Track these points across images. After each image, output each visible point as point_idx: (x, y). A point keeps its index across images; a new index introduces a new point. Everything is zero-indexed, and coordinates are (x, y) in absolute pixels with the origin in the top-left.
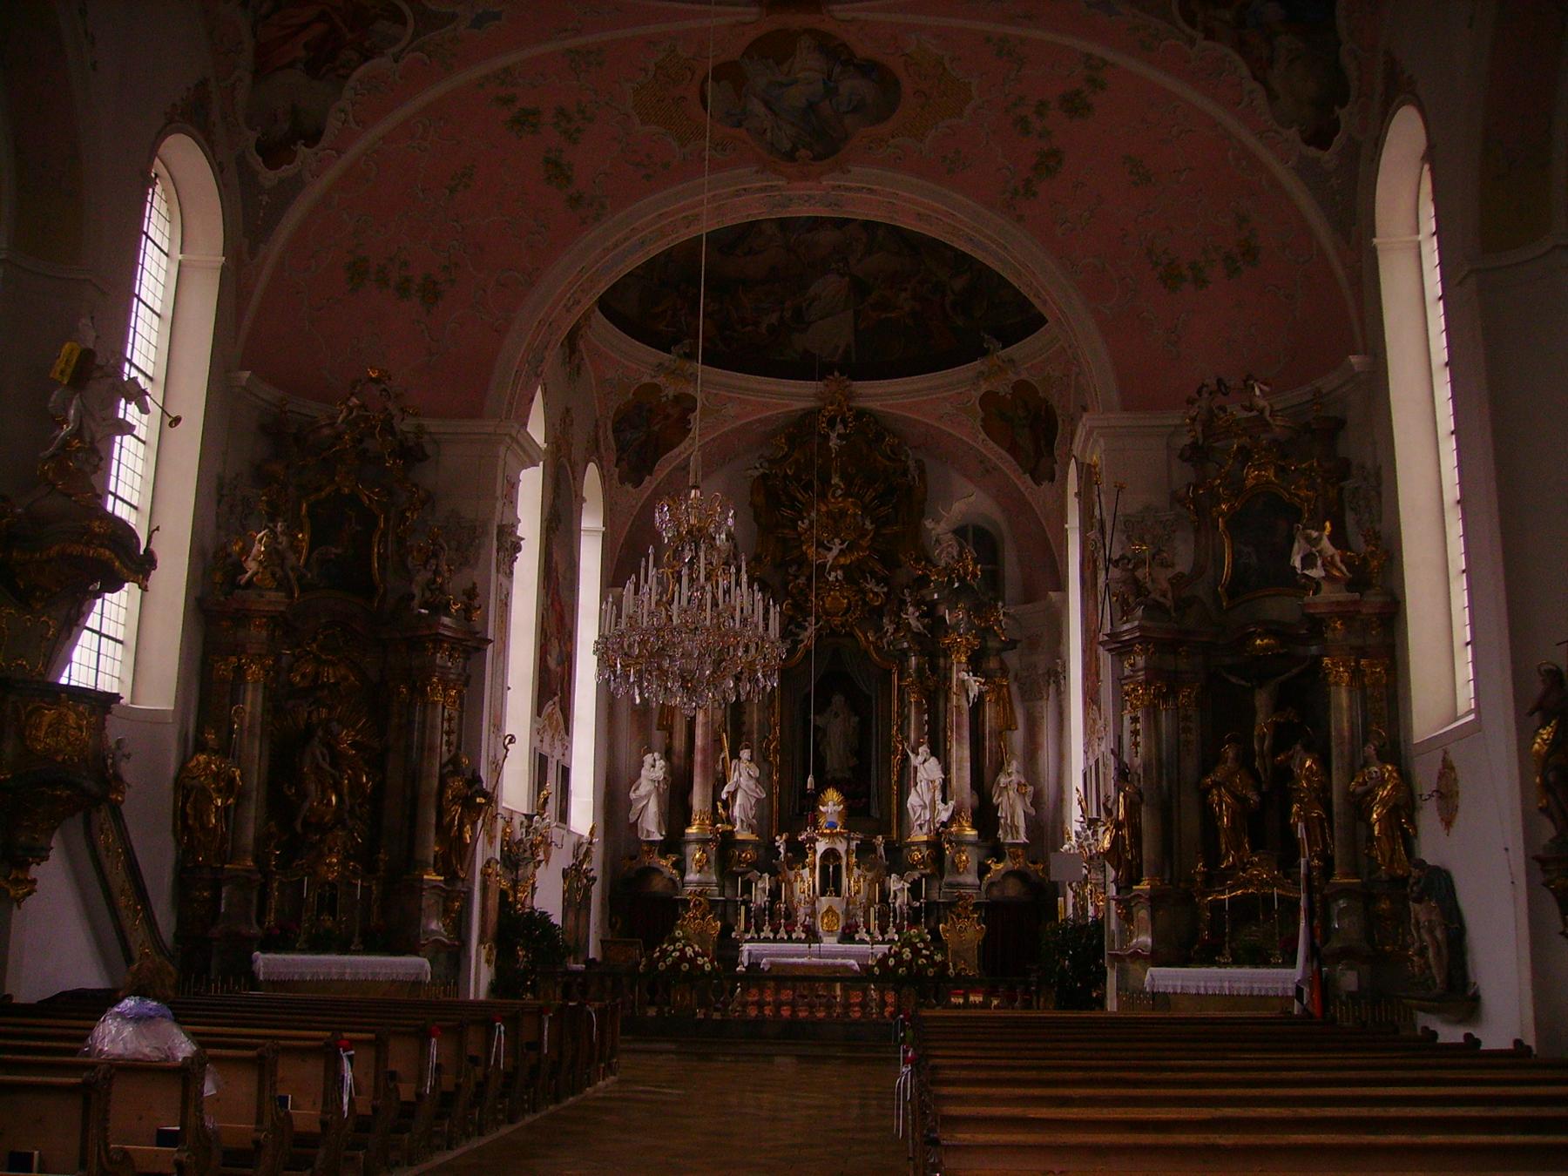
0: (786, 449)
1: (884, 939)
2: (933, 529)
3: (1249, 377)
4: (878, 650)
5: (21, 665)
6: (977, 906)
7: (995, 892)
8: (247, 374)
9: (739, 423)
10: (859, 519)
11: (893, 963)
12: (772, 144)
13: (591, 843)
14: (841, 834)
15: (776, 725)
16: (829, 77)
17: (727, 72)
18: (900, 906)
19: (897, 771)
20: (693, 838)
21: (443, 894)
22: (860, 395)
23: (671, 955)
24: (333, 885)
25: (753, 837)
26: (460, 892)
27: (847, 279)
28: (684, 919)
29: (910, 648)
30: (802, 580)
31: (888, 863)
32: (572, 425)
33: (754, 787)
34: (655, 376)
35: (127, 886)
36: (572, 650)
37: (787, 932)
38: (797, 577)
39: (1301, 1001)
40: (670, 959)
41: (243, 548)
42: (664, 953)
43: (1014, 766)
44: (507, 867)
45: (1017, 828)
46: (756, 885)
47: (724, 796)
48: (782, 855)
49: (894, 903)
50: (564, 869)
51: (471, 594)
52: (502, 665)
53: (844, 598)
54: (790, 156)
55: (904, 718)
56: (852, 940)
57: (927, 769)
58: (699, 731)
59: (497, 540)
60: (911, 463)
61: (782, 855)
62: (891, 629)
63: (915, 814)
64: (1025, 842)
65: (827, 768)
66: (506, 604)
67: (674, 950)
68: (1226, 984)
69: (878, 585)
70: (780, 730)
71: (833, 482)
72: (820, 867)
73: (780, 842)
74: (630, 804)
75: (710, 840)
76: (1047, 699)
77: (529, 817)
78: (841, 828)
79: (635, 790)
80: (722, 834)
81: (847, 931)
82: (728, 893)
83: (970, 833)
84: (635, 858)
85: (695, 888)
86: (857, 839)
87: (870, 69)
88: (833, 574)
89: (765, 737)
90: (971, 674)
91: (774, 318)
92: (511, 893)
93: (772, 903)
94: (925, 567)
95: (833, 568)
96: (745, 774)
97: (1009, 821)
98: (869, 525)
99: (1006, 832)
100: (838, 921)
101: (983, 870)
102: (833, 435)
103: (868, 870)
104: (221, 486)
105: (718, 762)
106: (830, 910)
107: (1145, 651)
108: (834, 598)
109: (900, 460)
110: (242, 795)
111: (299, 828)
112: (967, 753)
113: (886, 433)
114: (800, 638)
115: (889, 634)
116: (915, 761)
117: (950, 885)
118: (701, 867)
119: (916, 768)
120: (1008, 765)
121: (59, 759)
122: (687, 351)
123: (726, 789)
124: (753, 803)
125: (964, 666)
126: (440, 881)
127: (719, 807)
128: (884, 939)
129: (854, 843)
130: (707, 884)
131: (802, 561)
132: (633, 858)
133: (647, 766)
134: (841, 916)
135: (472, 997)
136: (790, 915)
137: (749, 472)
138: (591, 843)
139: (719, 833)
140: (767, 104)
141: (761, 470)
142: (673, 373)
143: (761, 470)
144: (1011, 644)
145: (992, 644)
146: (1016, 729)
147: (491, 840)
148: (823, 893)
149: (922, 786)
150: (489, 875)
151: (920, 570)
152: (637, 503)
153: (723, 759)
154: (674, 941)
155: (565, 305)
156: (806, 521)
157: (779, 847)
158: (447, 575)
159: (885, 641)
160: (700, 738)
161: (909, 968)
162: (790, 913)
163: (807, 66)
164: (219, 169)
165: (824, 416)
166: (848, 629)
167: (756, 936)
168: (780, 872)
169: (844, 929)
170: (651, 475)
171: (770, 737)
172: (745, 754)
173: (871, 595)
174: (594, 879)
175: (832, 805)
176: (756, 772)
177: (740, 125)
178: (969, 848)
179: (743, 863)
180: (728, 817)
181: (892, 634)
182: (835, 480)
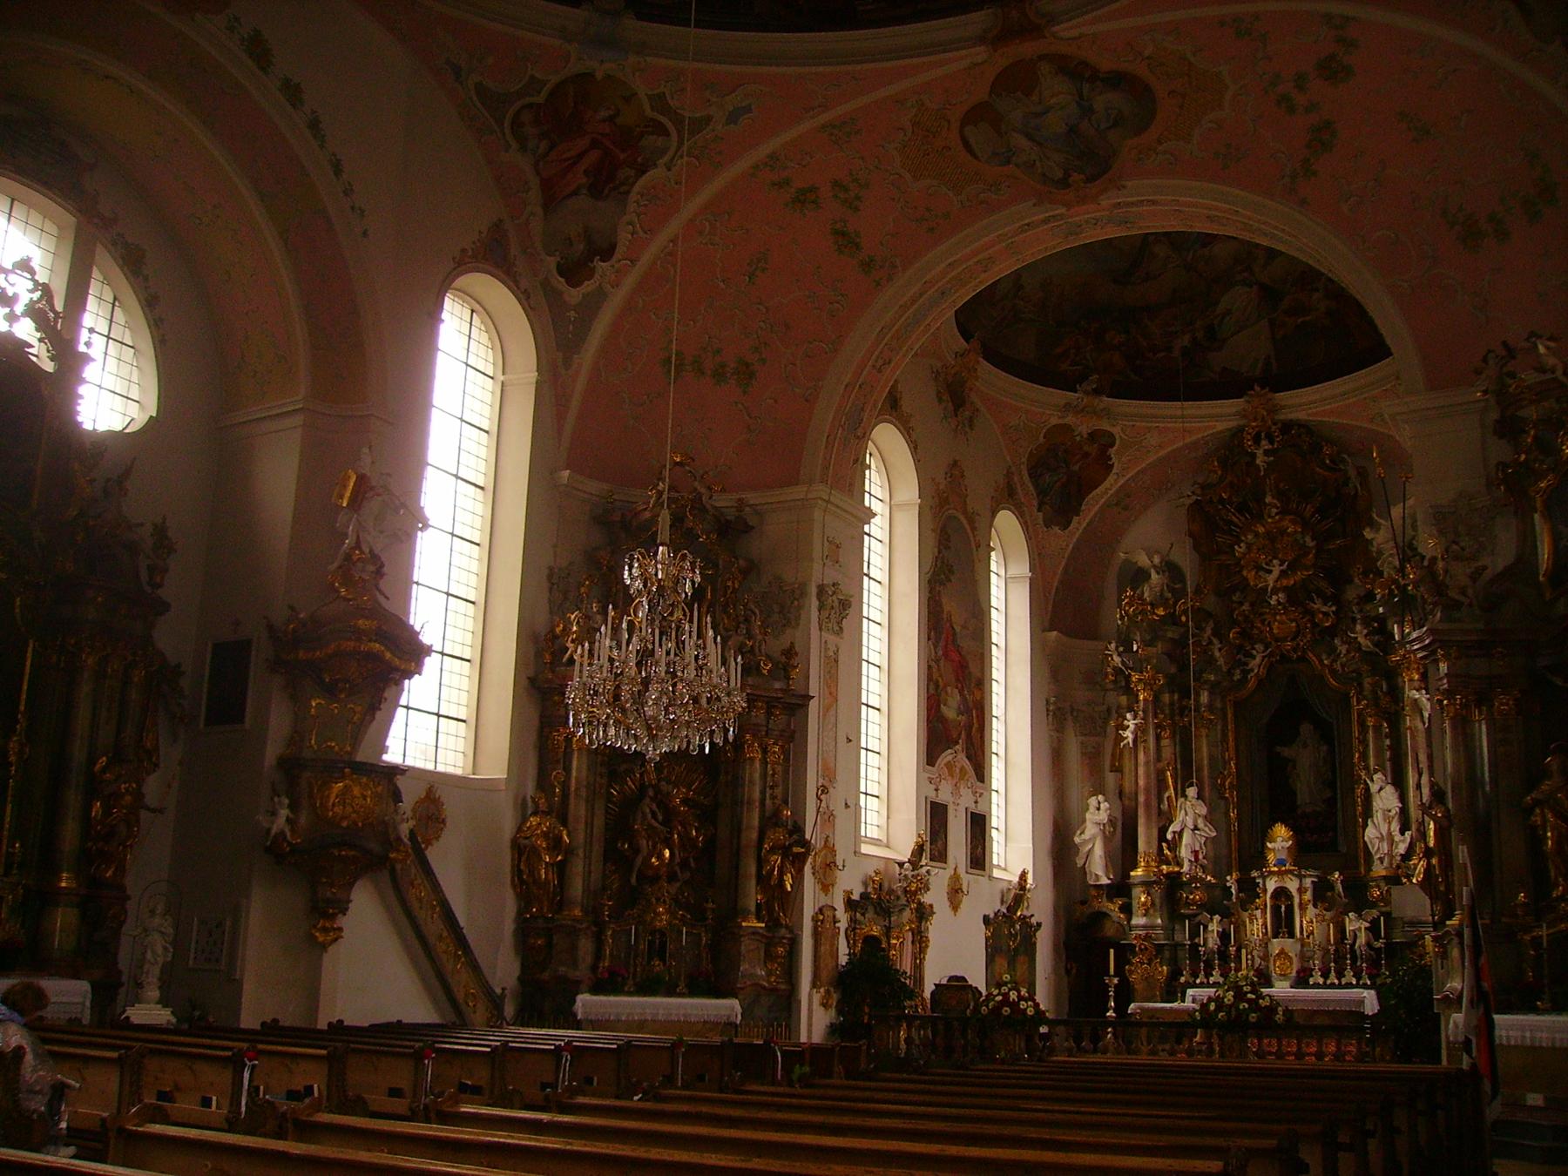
0: (1220, 472)
3: (1532, 334)
4: (1333, 672)
5: (330, 746)
8: (566, 473)
9: (1162, 453)
10: (1299, 536)
12: (1044, 175)
14: (1291, 872)
16: (1081, 96)
17: (978, 114)
20: (1136, 881)
21: (764, 940)
22: (1283, 407)
24: (663, 934)
26: (784, 938)
27: (1255, 287)
28: (1132, 964)
30: (1246, 607)
32: (963, 476)
34: (1063, 417)
35: (445, 934)
36: (983, 698)
38: (1241, 604)
39: (1469, 1053)
41: (564, 629)
44: (878, 915)
47: (1169, 836)
48: (1234, 897)
50: (985, 916)
51: (790, 652)
52: (833, 719)
53: (1292, 621)
54: (1064, 183)
56: (1305, 985)
57: (1385, 800)
59: (819, 599)
60: (1352, 473)
62: (1343, 649)
65: (1299, 803)
66: (836, 661)
67: (998, 995)
68: (1528, 1034)
69: (1325, 605)
70: (1236, 764)
71: (1267, 501)
72: (1271, 907)
73: (1231, 881)
74: (1075, 849)
75: (1155, 882)
77: (901, 865)
80: (1168, 875)
81: (1302, 975)
84: (1086, 903)
86: (1311, 876)
87: (1117, 80)
88: (1274, 597)
91: (1185, 340)
92: (884, 939)
95: (1275, 591)
100: (1291, 964)
102: (1260, 453)
103: (1326, 910)
104: (550, 577)
106: (1282, 952)
107: (1446, 657)
108: (1281, 622)
109: (1340, 470)
110: (569, 852)
111: (633, 881)
113: (1324, 443)
114: (1250, 666)
116: (1374, 788)
118: (1147, 910)
121: (344, 824)
123: (1171, 829)
125: (1416, 684)
126: (761, 928)
127: (1166, 845)
128: (1340, 983)
130: (1153, 927)
131: (1244, 586)
132: (1083, 903)
133: (1092, 809)
134: (1295, 960)
135: (803, 1039)
140: (1029, 136)
141: (1195, 497)
142: (1082, 410)
143: (1195, 497)
147: (826, 887)
148: (1275, 936)
149: (1378, 817)
150: (822, 921)
152: (1067, 546)
153: (1168, 798)
155: (874, 366)
158: (760, 637)
161: (1228, 1013)
163: (1056, 92)
164: (524, 298)
167: (1205, 981)
168: (1233, 914)
170: (1078, 515)
171: (1226, 773)
173: (1321, 616)
175: (1280, 839)
177: (1009, 163)
182: (1268, 500)
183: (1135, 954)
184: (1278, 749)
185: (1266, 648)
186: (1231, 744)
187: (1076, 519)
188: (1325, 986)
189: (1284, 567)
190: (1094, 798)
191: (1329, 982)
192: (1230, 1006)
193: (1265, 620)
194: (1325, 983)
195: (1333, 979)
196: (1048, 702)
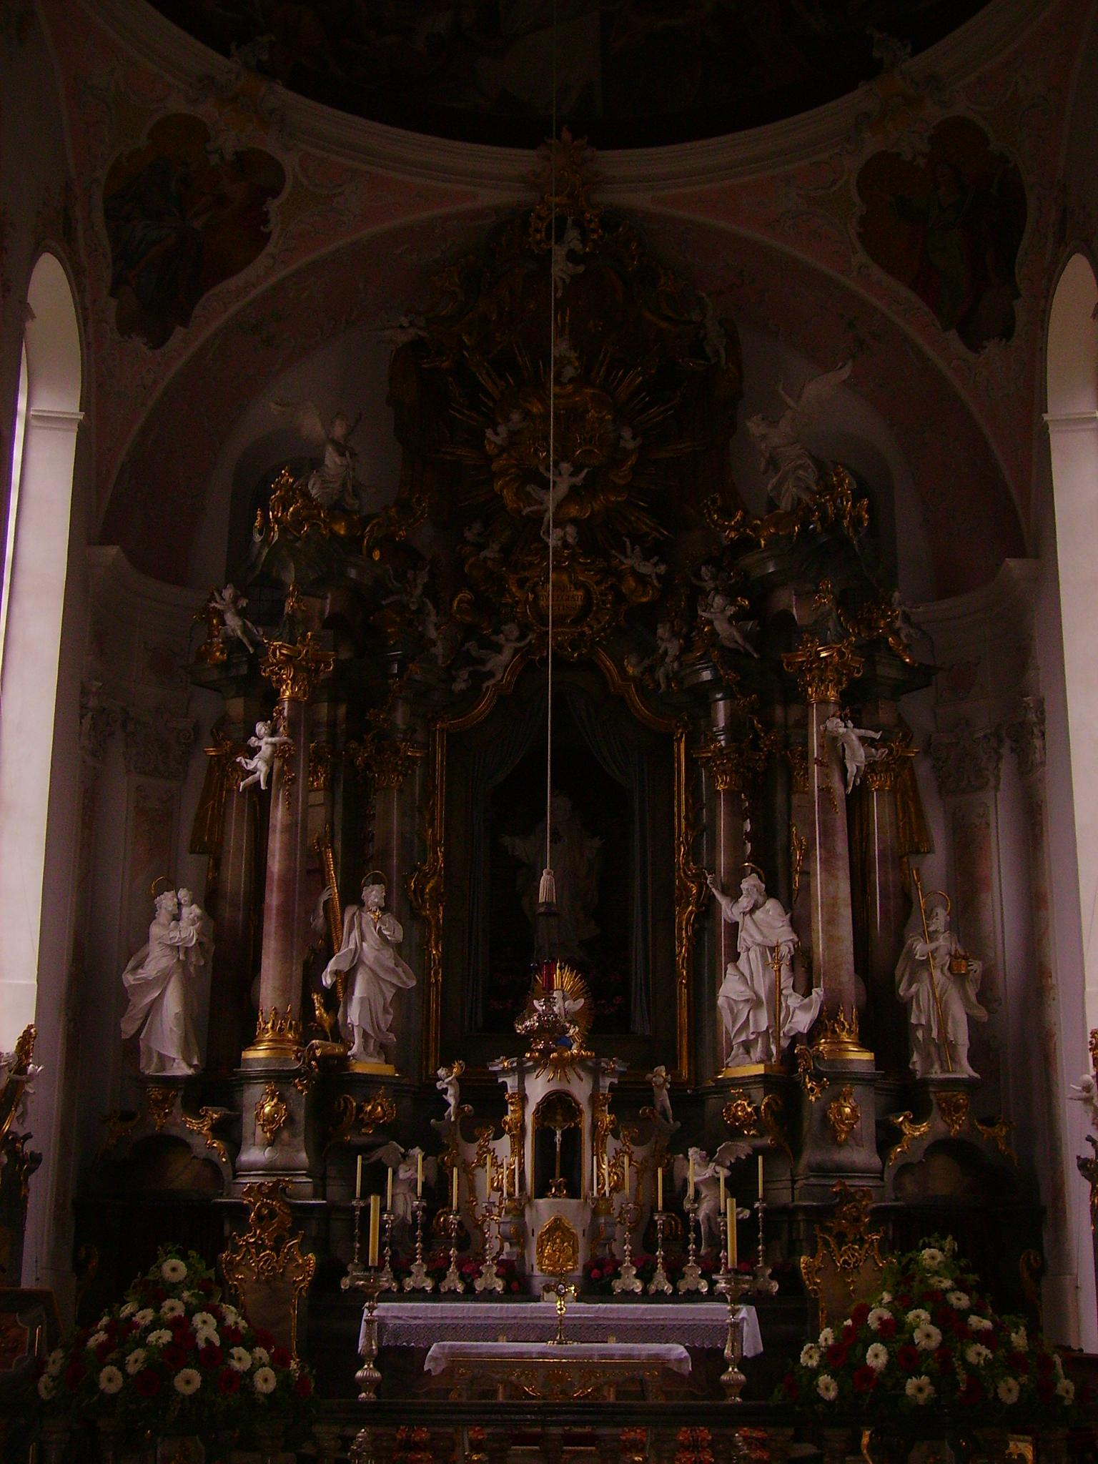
1: (676, 1290)
2: (764, 437)
6: (880, 1216)
7: (910, 1186)
11: (883, 1359)
13: (21, 1069)
15: (436, 843)
18: (708, 1218)
19: (688, 938)
23: (141, 1342)
25: (388, 1070)
28: (236, 1250)
29: (716, 684)
30: (492, 552)
31: (679, 1124)
33: (391, 963)
37: (462, 1278)
38: (481, 547)
40: (140, 1353)
42: (124, 1334)
43: (941, 918)
45: (952, 1047)
46: (395, 1173)
47: (327, 980)
48: (451, 1109)
49: (695, 1211)
55: (701, 830)
58: (276, 843)
61: (451, 1109)
62: (673, 648)
63: (734, 1021)
64: (971, 1078)
67: (156, 1325)
69: (646, 558)
70: (445, 854)
73: (447, 1080)
74: (123, 998)
75: (296, 1074)
76: (996, 788)
78: (581, 1047)
79: (135, 968)
80: (323, 1060)
82: (335, 1191)
83: (859, 1056)
85: (259, 1180)
89: (416, 869)
90: (850, 724)
93: (430, 1213)
94: (744, 523)
95: (559, 523)
96: (372, 936)
97: (934, 1034)
98: (630, 444)
99: (927, 1059)
100: (575, 1252)
101: (887, 1137)
102: (559, 252)
103: (636, 1142)
105: (315, 910)
106: (557, 1227)
112: (844, 888)
114: (489, 667)
115: (668, 660)
116: (729, 911)
117: (821, 1170)
119: (734, 928)
120: (929, 917)
122: (265, 57)
123: (331, 966)
124: (390, 996)
125: (832, 709)
128: (676, 1290)
129: (607, 1082)
130: (289, 1169)
133: (163, 917)
134: (581, 1242)
136: (469, 1238)
137: (387, 332)
138: (21, 1069)
139: (315, 1059)
141: (412, 331)
143: (412, 331)
144: (919, 677)
145: (886, 671)
146: (930, 851)
148: (541, 1191)
149: (751, 960)
151: (732, 528)
153: (326, 903)
154: (157, 1294)
156: (502, 430)
157: (445, 1091)
159: (660, 674)
160: (277, 858)
162: (468, 1235)
165: (539, 217)
166: (584, 651)
169: (587, 1269)
170: (185, 322)
171: (426, 868)
172: (373, 894)
174: (36, 1159)
176: (394, 931)
178: (858, 1090)
179: (367, 1125)
180: (335, 1025)
181: (677, 658)
182: (559, 348)
183: (244, 1227)
184: (507, 840)
185: (522, 637)
186: (440, 812)
187: (179, 332)
188: (646, 1297)
189: (578, 480)
190: (169, 895)
191: (652, 1288)
192: (944, 1351)
193: (527, 579)
194: (645, 1291)
195: (661, 1282)
196: (84, 692)
